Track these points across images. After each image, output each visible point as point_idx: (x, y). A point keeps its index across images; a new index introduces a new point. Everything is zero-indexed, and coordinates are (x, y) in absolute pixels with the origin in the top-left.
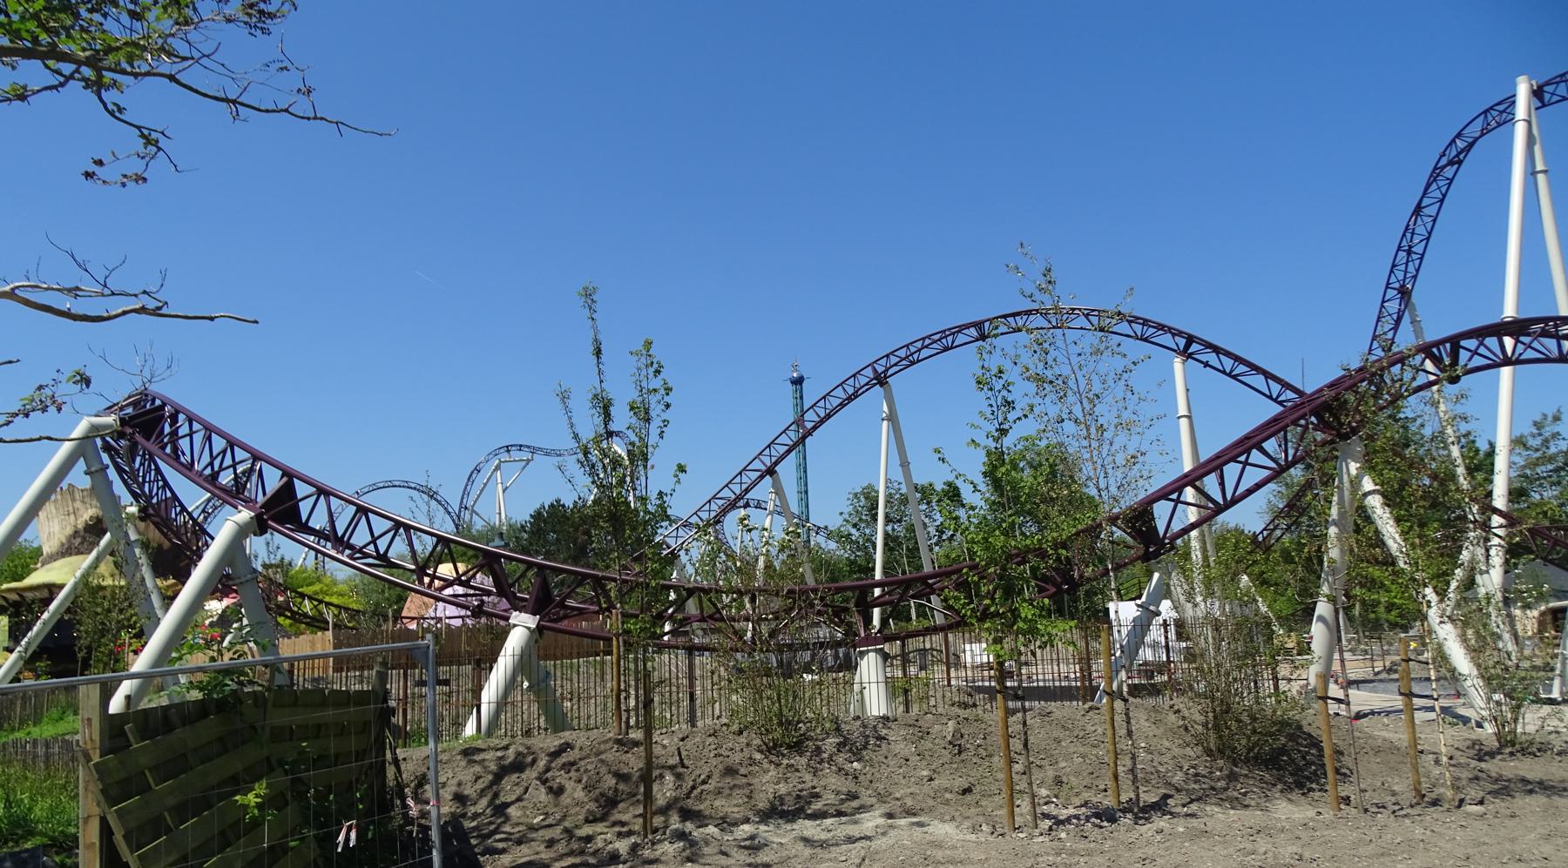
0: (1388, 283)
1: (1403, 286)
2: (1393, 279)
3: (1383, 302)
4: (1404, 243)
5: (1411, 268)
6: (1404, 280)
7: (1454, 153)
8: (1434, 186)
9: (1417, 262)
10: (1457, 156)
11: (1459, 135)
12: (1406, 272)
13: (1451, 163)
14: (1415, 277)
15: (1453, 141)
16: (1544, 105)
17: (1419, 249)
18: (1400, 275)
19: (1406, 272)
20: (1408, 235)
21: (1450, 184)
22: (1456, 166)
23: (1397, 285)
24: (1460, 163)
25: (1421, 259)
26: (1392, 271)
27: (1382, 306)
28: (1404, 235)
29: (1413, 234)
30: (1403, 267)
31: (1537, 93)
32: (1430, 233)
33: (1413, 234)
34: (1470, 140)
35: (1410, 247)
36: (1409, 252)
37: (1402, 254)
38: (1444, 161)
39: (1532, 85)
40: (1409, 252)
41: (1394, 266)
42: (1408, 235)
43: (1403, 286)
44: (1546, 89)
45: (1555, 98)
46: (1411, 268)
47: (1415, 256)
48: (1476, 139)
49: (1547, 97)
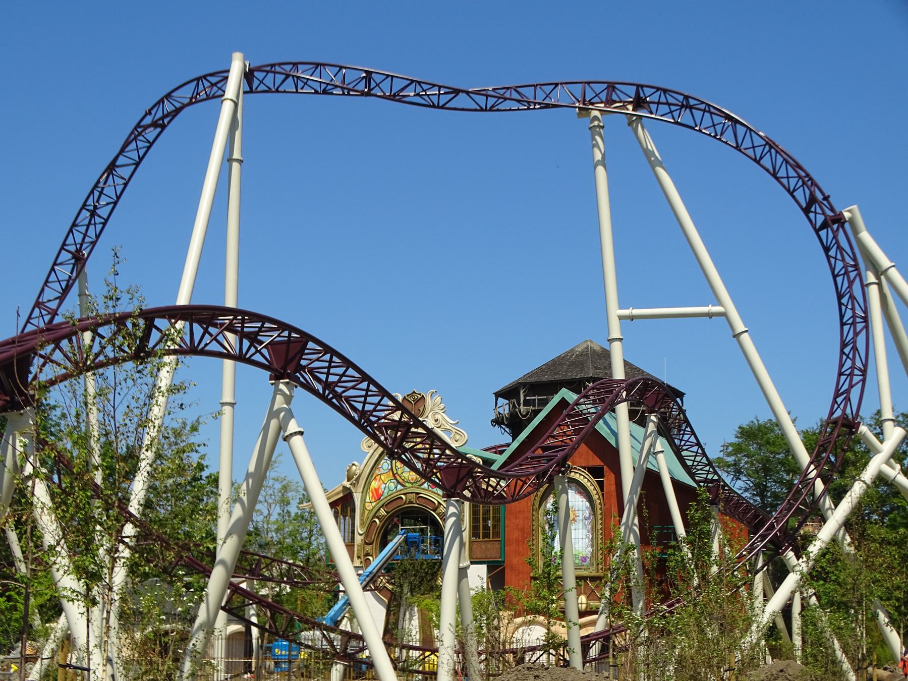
0: (64, 244)
1: (79, 251)
2: (70, 240)
3: (55, 264)
4: (90, 202)
5: (91, 233)
6: (81, 245)
7: (159, 114)
8: (133, 146)
9: (99, 227)
10: (162, 118)
11: (168, 96)
12: (85, 235)
13: (154, 124)
14: (94, 244)
15: (161, 101)
16: (251, 91)
17: (103, 212)
18: (79, 238)
19: (85, 235)
20: (96, 194)
21: (149, 148)
22: (159, 130)
23: (73, 248)
24: (163, 127)
25: (104, 224)
26: (71, 231)
27: (53, 269)
28: (92, 192)
29: (101, 193)
30: (83, 229)
31: (248, 75)
32: (118, 198)
33: (101, 193)
34: (178, 105)
35: (95, 207)
36: (93, 214)
37: (86, 214)
38: (148, 120)
39: (245, 66)
40: (93, 214)
41: (74, 225)
42: (96, 194)
43: (79, 251)
44: (256, 74)
45: (262, 87)
46: (91, 233)
47: (98, 220)
48: (184, 106)
49: (256, 83)
